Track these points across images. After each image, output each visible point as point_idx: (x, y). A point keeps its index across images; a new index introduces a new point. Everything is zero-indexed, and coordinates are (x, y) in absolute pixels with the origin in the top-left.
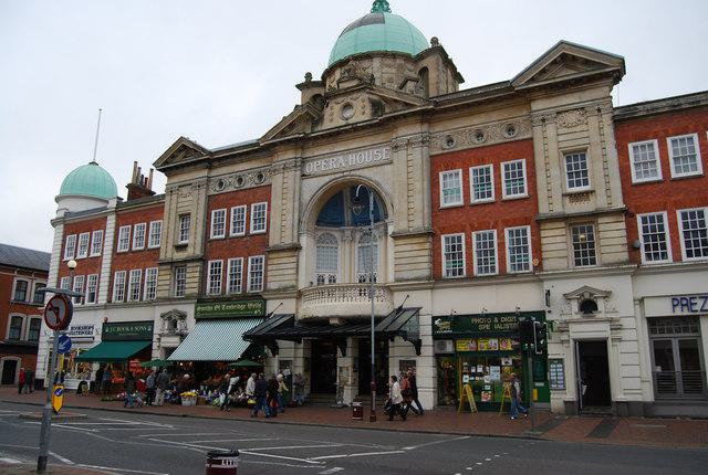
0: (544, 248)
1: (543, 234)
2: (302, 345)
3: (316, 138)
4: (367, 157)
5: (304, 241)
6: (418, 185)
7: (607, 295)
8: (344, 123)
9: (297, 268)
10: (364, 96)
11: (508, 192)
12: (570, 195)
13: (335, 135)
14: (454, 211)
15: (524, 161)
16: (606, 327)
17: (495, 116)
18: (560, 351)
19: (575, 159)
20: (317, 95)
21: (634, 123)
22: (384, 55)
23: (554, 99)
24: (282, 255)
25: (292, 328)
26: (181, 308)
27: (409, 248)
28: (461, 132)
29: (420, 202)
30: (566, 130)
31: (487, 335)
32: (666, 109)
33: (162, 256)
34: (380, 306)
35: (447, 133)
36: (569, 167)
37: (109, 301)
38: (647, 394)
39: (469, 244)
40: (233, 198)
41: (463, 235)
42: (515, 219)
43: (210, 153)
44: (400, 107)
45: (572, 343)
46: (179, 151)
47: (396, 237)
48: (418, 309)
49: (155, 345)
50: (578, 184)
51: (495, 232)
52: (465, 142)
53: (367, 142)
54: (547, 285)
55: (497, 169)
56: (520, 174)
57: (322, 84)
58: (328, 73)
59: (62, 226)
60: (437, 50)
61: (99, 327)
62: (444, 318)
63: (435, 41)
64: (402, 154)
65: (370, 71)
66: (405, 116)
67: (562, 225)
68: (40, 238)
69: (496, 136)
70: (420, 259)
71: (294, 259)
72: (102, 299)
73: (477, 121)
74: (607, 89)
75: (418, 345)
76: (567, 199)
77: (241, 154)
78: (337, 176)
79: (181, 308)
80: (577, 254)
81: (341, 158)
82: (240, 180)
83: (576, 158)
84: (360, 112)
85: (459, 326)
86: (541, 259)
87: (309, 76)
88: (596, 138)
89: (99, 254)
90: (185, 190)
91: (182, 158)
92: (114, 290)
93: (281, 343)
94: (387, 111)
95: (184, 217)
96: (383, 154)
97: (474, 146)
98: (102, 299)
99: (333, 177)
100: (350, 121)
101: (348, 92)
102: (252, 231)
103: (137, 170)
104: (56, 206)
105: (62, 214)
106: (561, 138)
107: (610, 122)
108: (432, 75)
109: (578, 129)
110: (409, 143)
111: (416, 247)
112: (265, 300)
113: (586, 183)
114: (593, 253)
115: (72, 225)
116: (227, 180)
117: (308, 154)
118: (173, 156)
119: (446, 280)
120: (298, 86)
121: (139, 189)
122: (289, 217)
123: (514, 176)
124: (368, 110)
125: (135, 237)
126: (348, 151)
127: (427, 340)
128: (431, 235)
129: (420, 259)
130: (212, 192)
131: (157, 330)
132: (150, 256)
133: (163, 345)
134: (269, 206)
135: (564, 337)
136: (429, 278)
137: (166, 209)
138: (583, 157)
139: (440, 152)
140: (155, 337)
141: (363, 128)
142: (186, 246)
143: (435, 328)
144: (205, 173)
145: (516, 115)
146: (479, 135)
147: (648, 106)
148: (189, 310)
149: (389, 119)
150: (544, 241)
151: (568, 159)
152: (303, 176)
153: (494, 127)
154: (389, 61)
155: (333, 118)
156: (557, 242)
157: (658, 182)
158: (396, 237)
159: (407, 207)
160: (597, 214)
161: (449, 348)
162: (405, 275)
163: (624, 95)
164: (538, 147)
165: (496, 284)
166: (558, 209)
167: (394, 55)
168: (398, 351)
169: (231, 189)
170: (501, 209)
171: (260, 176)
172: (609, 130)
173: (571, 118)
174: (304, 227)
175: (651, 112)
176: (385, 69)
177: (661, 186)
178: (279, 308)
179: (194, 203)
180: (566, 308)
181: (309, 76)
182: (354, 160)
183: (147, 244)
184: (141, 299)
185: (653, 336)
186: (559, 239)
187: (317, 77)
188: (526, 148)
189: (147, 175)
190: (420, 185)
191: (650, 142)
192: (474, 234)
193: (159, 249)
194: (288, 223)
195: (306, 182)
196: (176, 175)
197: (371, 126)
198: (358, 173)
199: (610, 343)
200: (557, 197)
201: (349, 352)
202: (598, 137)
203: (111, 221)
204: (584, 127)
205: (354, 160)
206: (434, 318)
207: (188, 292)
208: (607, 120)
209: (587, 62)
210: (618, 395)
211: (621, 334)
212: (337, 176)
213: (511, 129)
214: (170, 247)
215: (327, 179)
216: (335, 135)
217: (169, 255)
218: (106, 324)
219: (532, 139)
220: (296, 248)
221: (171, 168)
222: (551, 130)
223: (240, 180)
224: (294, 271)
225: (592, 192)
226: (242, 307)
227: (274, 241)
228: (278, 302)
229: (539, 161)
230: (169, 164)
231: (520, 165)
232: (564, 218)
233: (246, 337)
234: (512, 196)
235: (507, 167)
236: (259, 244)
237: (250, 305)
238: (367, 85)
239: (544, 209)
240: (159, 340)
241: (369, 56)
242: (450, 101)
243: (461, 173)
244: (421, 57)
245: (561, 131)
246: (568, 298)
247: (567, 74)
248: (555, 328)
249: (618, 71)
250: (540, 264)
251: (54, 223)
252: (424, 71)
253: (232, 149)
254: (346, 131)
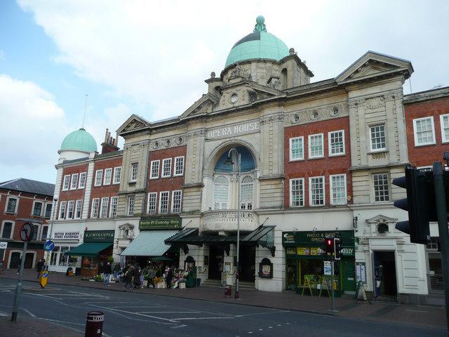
0: (354, 189)
1: (354, 179)
2: (203, 248)
3: (214, 115)
4: (245, 128)
5: (206, 181)
6: (276, 147)
8: (232, 106)
9: (201, 199)
10: (244, 88)
11: (333, 152)
12: (373, 154)
13: (225, 114)
14: (298, 164)
15: (343, 131)
16: (394, 242)
17: (325, 101)
18: (362, 256)
19: (378, 131)
20: (219, 85)
21: (416, 106)
22: (259, 61)
23: (364, 90)
24: (192, 190)
25: (196, 237)
26: (131, 222)
27: (269, 187)
28: (304, 112)
29: (277, 158)
30: (371, 111)
31: (315, 245)
32: (440, 96)
33: (121, 190)
34: (249, 224)
35: (295, 113)
36: (373, 135)
37: (89, 217)
38: (423, 289)
39: (307, 185)
40: (164, 153)
41: (303, 179)
42: (336, 170)
43: (150, 125)
44: (265, 96)
45: (371, 252)
46: (132, 123)
47: (261, 180)
48: (273, 227)
49: (115, 246)
50: (379, 147)
51: (323, 177)
52: (304, 120)
53: (245, 118)
54: (356, 214)
55: (326, 137)
56: (341, 140)
57: (221, 79)
58: (224, 73)
59: (62, 169)
60: (293, 57)
61: (82, 233)
62: (290, 233)
63: (292, 50)
64: (266, 127)
65: (249, 72)
66: (268, 102)
67: (367, 173)
68: (48, 175)
69: (326, 114)
70: (275, 195)
71: (199, 193)
72: (85, 216)
73: (314, 105)
74: (399, 83)
75: (273, 250)
76: (371, 156)
77: (169, 126)
78: (227, 140)
79: (131, 222)
80: (377, 194)
81: (229, 129)
82: (168, 142)
83: (377, 130)
84: (241, 98)
85: (298, 239)
86: (352, 196)
87: (213, 74)
88: (390, 116)
89: (83, 187)
90: (135, 148)
91: (134, 128)
92: (92, 208)
93: (190, 246)
94: (258, 98)
95: (135, 165)
96: (255, 126)
97: (311, 121)
98: (85, 216)
99: (224, 140)
100: (236, 105)
101: (234, 86)
102: (175, 175)
103: (108, 134)
104: (58, 156)
105: (61, 162)
106: (368, 116)
107: (401, 105)
108: (290, 73)
109: (379, 109)
110: (271, 120)
111: (274, 187)
112: (181, 219)
113: (384, 146)
114: (387, 193)
115: (71, 169)
116: (160, 142)
117: (209, 126)
118: (128, 127)
119: (292, 209)
120: (206, 81)
121: (109, 147)
122: (197, 166)
123: (336, 140)
124: (247, 98)
125: (108, 177)
126: (234, 124)
127: (279, 248)
129: (275, 195)
130: (151, 149)
131: (116, 236)
132: (113, 190)
133: (119, 245)
134: (185, 159)
135: (366, 248)
136: (281, 207)
137: (124, 160)
138: (382, 129)
139: (291, 125)
140: (115, 240)
141: (243, 109)
142: (135, 183)
143: (284, 239)
144: (147, 137)
145: (339, 101)
146: (316, 114)
147: (427, 94)
148: (136, 223)
149: (258, 104)
150: (354, 184)
151: (373, 130)
153: (324, 108)
154: (262, 65)
155: (226, 102)
156: (365, 186)
157: (433, 145)
158: (261, 180)
159: (269, 161)
160: (389, 167)
161: (292, 252)
162: (266, 205)
163: (411, 87)
164: (352, 122)
165: (322, 212)
166: (364, 163)
167: (265, 61)
168: (261, 253)
169: (163, 147)
170: (328, 163)
171: (181, 139)
172: (400, 111)
173: (375, 102)
174: (205, 172)
175: (429, 98)
176: (259, 70)
177: (435, 148)
178: (189, 223)
179: (141, 155)
180: (368, 229)
181: (213, 74)
182: (237, 129)
183: (112, 181)
184: (108, 216)
185: (428, 250)
186: (364, 183)
187: (218, 76)
188: (344, 123)
189: (114, 137)
190: (278, 147)
191: (429, 118)
192: (310, 179)
193: (119, 185)
194: (196, 170)
195: (207, 144)
196: (130, 138)
197: (248, 108)
198: (239, 138)
199: (397, 254)
200: (364, 156)
201: (231, 252)
202: (394, 115)
203: (91, 166)
204: (383, 108)
205: (237, 129)
206: (284, 233)
207: (135, 212)
208: (399, 103)
209: (386, 65)
210: (402, 288)
211: (404, 247)
212: (227, 140)
213: (336, 110)
214: (126, 183)
215: (220, 142)
216: (225, 114)
217: (125, 189)
218: (86, 232)
219: (348, 117)
220: (200, 186)
221: (127, 134)
222: (361, 111)
223: (168, 142)
224: (199, 201)
225: (387, 152)
226: (167, 223)
227: (188, 181)
228: (189, 220)
229: (353, 131)
230: (125, 132)
231: (341, 134)
232: (368, 169)
233: (167, 242)
234: (336, 154)
235: (332, 135)
236: (179, 183)
237: (172, 222)
238: (245, 81)
239: (355, 163)
240: (117, 242)
241: (249, 62)
242: (297, 92)
243: (323, 137)
244: (283, 61)
245: (368, 111)
246: (368, 222)
247: (371, 73)
248: (360, 242)
249: (407, 70)
250: (352, 199)
251: (57, 167)
252: (285, 71)
253: (163, 123)
254: (233, 111)
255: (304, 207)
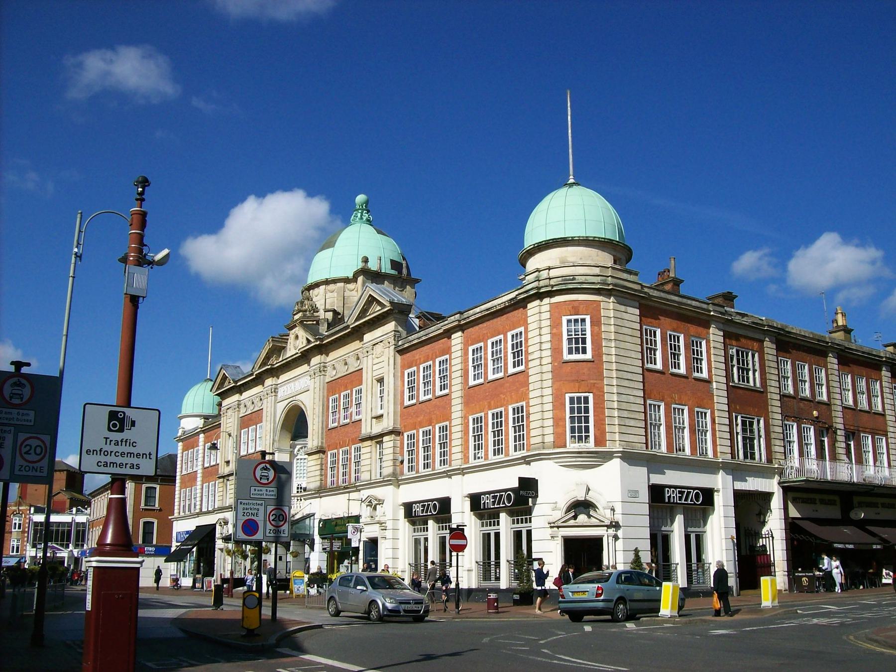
7: (381, 502)
22: (327, 282)
48: (313, 515)
106: (375, 367)
117: (280, 381)
127: (317, 538)
128: (321, 451)
152: (276, 402)
154: (332, 287)
167: (335, 281)
176: (329, 295)
190: (319, 409)
198: (298, 397)
232: (371, 438)
255: (336, 490)
